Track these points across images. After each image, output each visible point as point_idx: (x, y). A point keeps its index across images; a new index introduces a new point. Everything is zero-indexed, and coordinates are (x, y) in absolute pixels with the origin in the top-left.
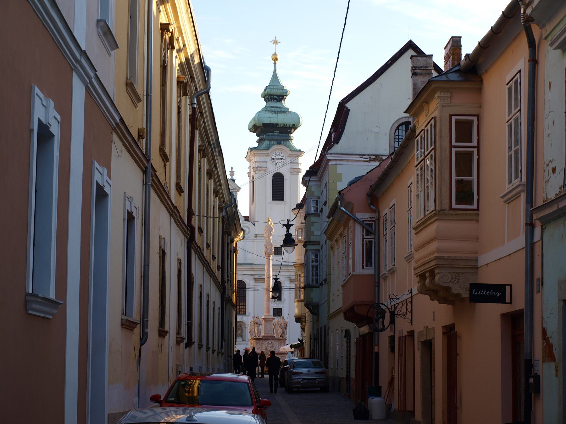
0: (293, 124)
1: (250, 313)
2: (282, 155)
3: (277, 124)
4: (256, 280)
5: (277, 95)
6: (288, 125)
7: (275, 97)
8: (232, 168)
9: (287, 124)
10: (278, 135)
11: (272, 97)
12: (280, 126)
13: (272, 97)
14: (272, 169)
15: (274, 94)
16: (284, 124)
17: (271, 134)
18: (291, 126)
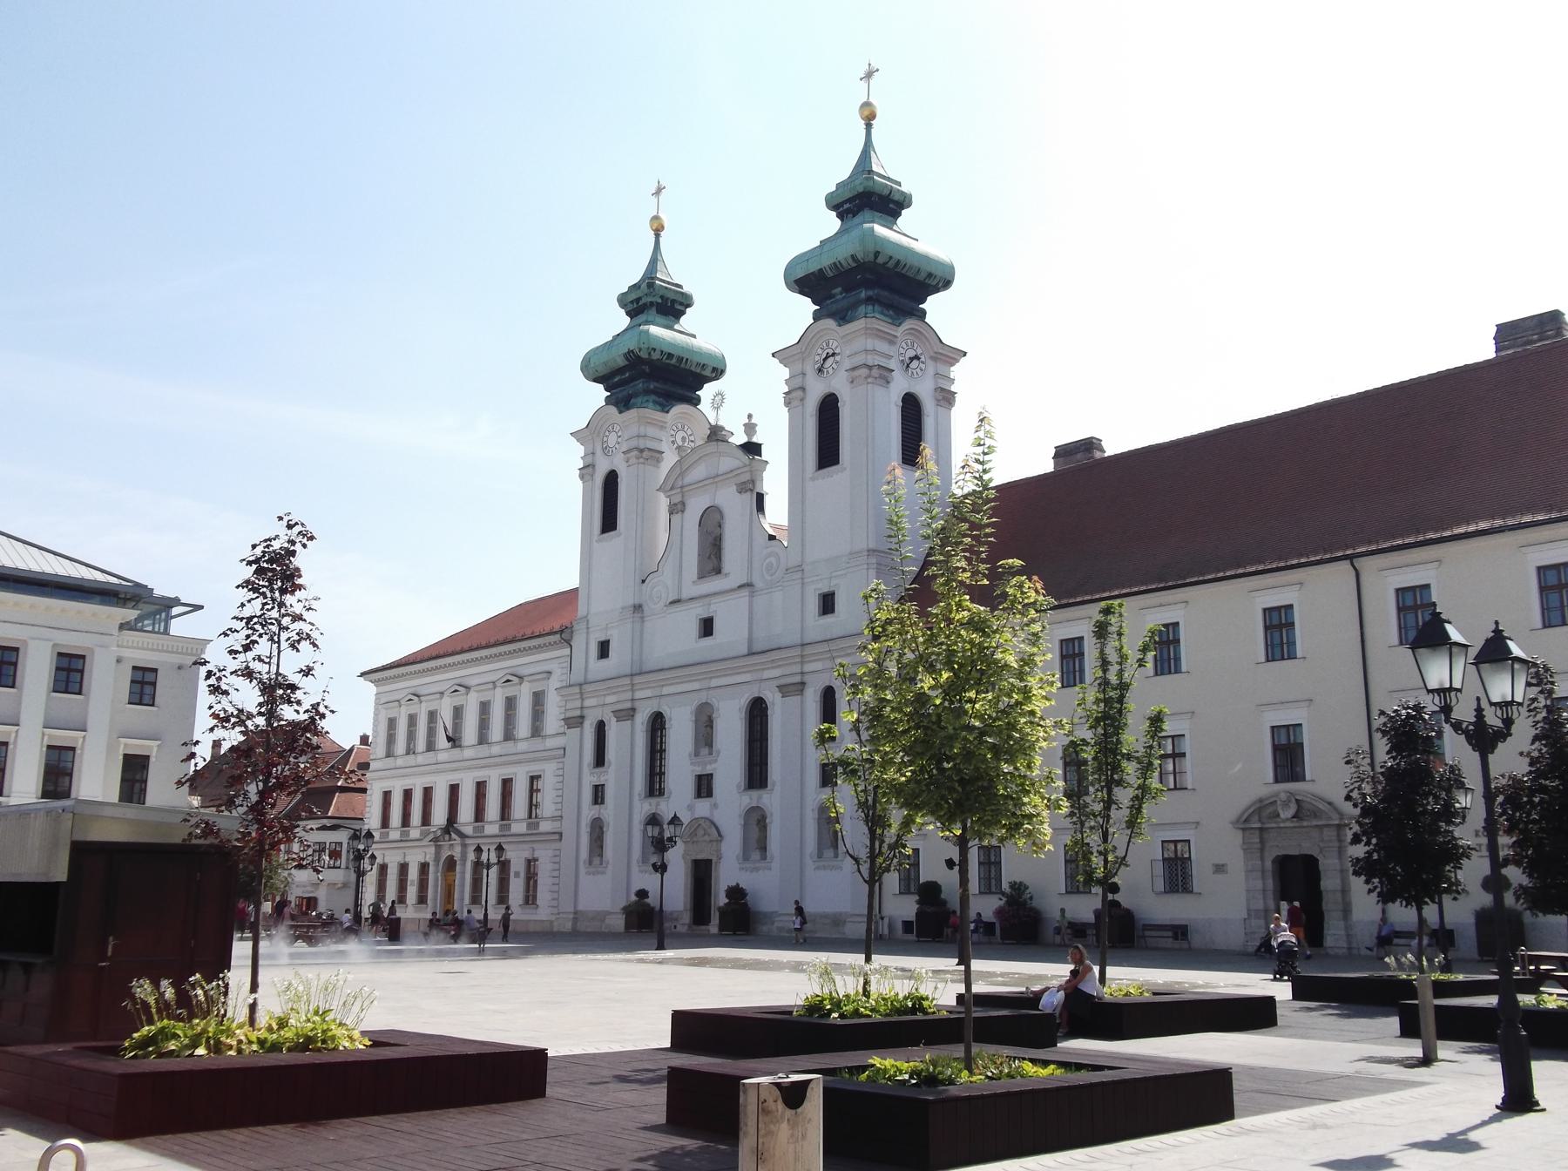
0: (852, 255)
1: (774, 785)
2: (835, 344)
3: (821, 269)
4: (785, 690)
5: (849, 200)
6: (844, 264)
7: (846, 206)
8: (750, 416)
9: (839, 262)
10: (844, 298)
11: (841, 209)
12: (831, 274)
13: (841, 209)
14: (816, 391)
15: (841, 200)
16: (835, 263)
17: (828, 302)
18: (854, 265)
